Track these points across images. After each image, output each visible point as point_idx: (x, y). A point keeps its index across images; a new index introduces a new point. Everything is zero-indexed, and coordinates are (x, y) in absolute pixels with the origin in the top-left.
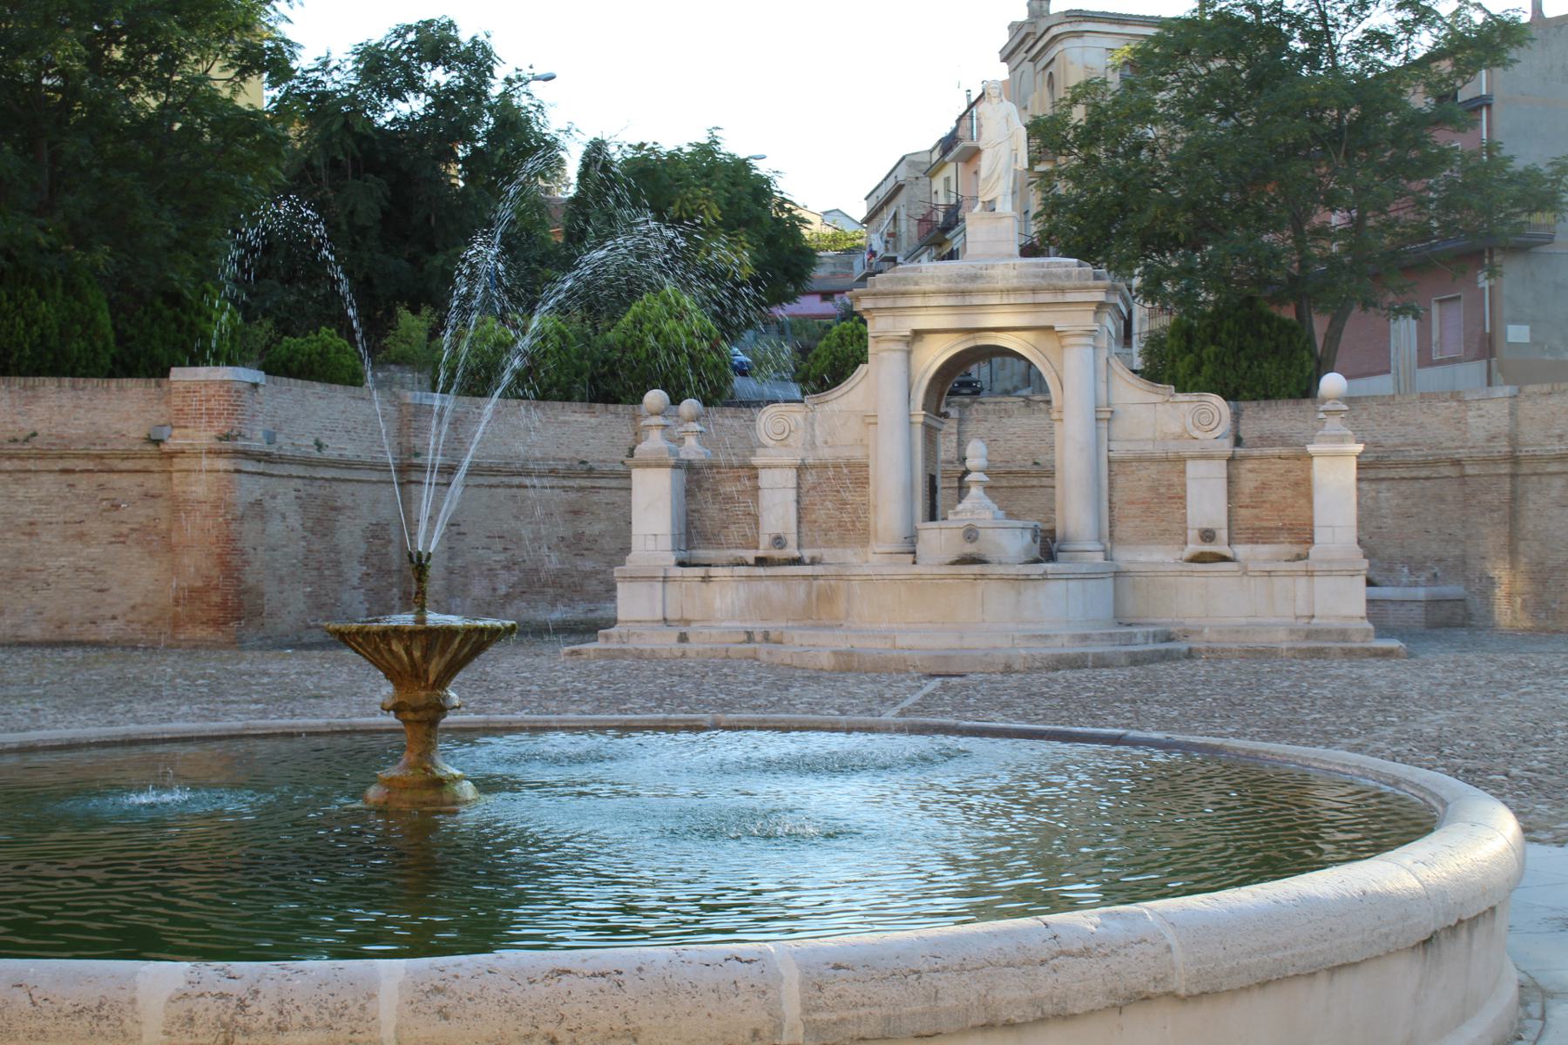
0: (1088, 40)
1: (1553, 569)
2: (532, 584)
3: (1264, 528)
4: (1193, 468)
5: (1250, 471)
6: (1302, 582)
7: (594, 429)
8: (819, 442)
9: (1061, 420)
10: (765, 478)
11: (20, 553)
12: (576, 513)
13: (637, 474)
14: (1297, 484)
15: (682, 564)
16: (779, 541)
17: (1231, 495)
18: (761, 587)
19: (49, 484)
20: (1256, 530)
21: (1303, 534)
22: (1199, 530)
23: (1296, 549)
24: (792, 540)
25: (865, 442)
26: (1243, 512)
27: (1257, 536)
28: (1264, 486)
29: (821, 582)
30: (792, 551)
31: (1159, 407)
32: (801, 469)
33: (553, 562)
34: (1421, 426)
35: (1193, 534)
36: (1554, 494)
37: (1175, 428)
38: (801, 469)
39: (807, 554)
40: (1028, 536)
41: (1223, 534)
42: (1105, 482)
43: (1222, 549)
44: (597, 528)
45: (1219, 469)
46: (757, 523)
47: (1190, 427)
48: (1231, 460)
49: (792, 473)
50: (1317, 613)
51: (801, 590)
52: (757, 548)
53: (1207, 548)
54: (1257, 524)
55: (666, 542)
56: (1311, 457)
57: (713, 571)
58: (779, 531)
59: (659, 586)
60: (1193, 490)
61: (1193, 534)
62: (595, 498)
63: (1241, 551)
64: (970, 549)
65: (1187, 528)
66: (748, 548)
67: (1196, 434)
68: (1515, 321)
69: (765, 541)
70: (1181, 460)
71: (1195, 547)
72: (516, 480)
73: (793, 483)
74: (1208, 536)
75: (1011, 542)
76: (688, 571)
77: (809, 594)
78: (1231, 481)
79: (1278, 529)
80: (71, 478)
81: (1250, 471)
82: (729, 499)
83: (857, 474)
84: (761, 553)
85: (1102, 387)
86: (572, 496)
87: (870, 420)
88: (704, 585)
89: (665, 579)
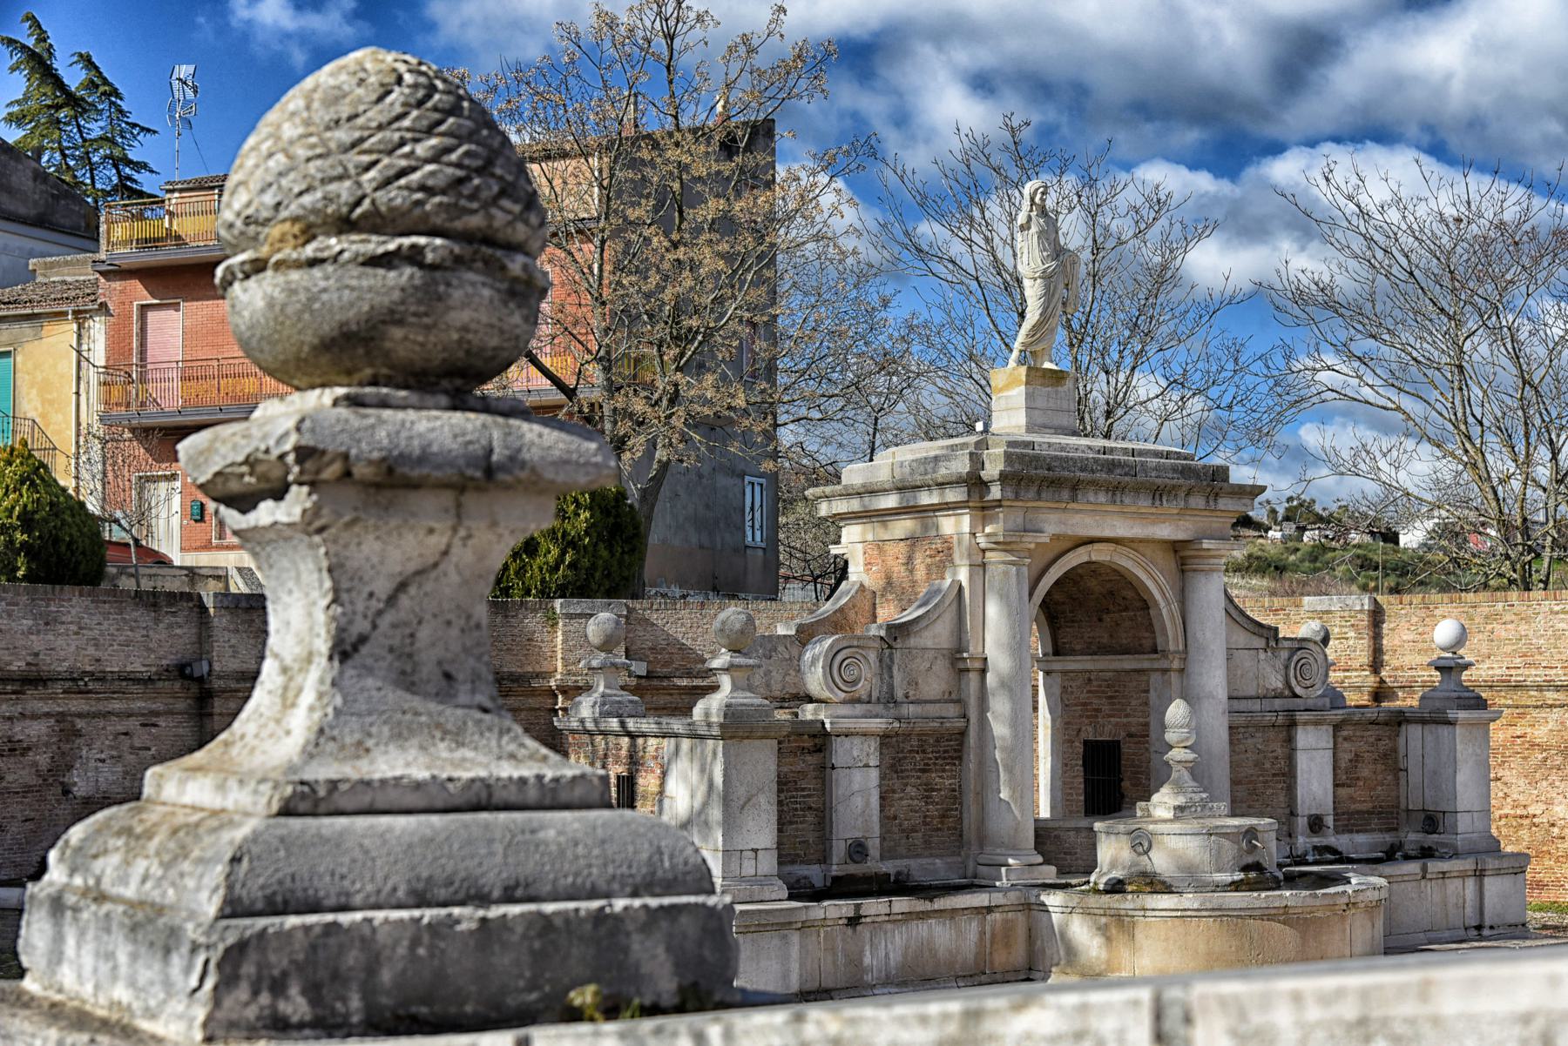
3: (1358, 812)
5: (1345, 739)
6: (1471, 883)
8: (899, 694)
9: (1182, 671)
10: (842, 752)
14: (1385, 756)
16: (858, 850)
18: (921, 929)
22: (1310, 817)
24: (874, 846)
25: (954, 696)
29: (997, 916)
30: (875, 864)
31: (1262, 655)
32: (885, 739)
35: (1302, 822)
37: (1276, 682)
38: (885, 739)
39: (889, 867)
41: (1329, 820)
49: (873, 744)
50: (1487, 923)
51: (972, 929)
52: (824, 859)
53: (1317, 841)
54: (1353, 807)
56: (1451, 723)
57: (873, 907)
58: (858, 834)
60: (1302, 760)
61: (1302, 822)
64: (1250, 860)
65: (1293, 814)
66: (809, 863)
69: (839, 850)
70: (1292, 725)
74: (1316, 824)
77: (982, 933)
79: (1368, 812)
81: (1345, 739)
84: (835, 870)
88: (849, 931)
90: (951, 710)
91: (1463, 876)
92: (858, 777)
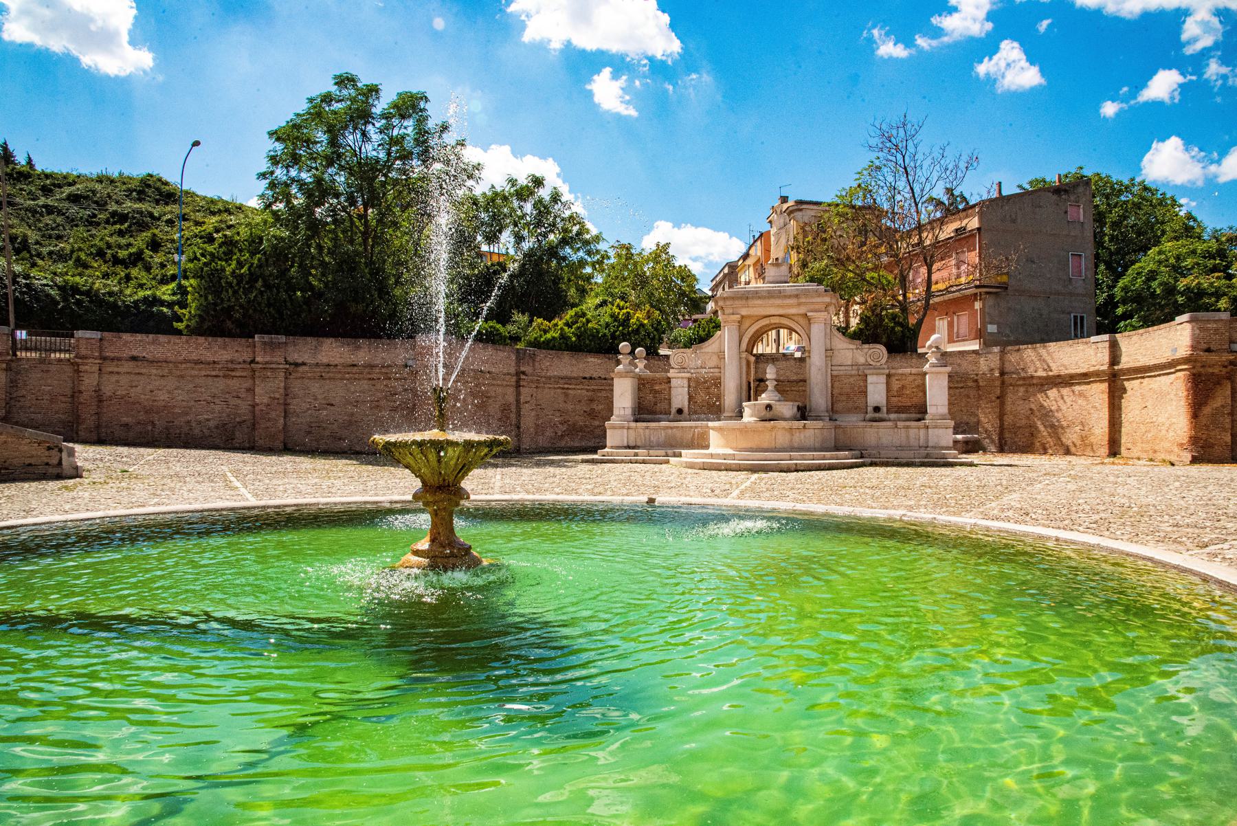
0: (804, 213)
1: (1020, 427)
2: (573, 430)
4: (870, 379)
6: (922, 432)
7: (599, 365)
10: (674, 382)
11: (352, 414)
12: (591, 400)
13: (616, 381)
15: (636, 421)
17: (888, 390)
19: (365, 384)
20: (899, 407)
21: (921, 411)
23: (919, 416)
26: (893, 399)
27: (900, 410)
28: (903, 387)
32: (689, 379)
33: (581, 421)
34: (959, 365)
35: (870, 409)
36: (1020, 394)
38: (689, 379)
40: (795, 409)
41: (885, 409)
42: (830, 385)
43: (883, 414)
44: (601, 407)
45: (883, 379)
46: (670, 404)
47: (869, 360)
48: (889, 376)
49: (685, 383)
53: (877, 415)
55: (629, 412)
59: (625, 431)
60: (870, 388)
61: (870, 409)
62: (599, 394)
63: (893, 416)
64: (769, 415)
67: (872, 363)
68: (990, 323)
69: (673, 411)
71: (870, 415)
72: (566, 386)
73: (686, 385)
74: (877, 409)
75: (787, 409)
76: (639, 424)
78: (888, 384)
80: (373, 382)
82: (656, 392)
83: (717, 382)
85: (828, 341)
86: (589, 394)
87: (720, 355)
89: (628, 428)
90: (717, 370)
91: (919, 428)
92: (680, 390)
